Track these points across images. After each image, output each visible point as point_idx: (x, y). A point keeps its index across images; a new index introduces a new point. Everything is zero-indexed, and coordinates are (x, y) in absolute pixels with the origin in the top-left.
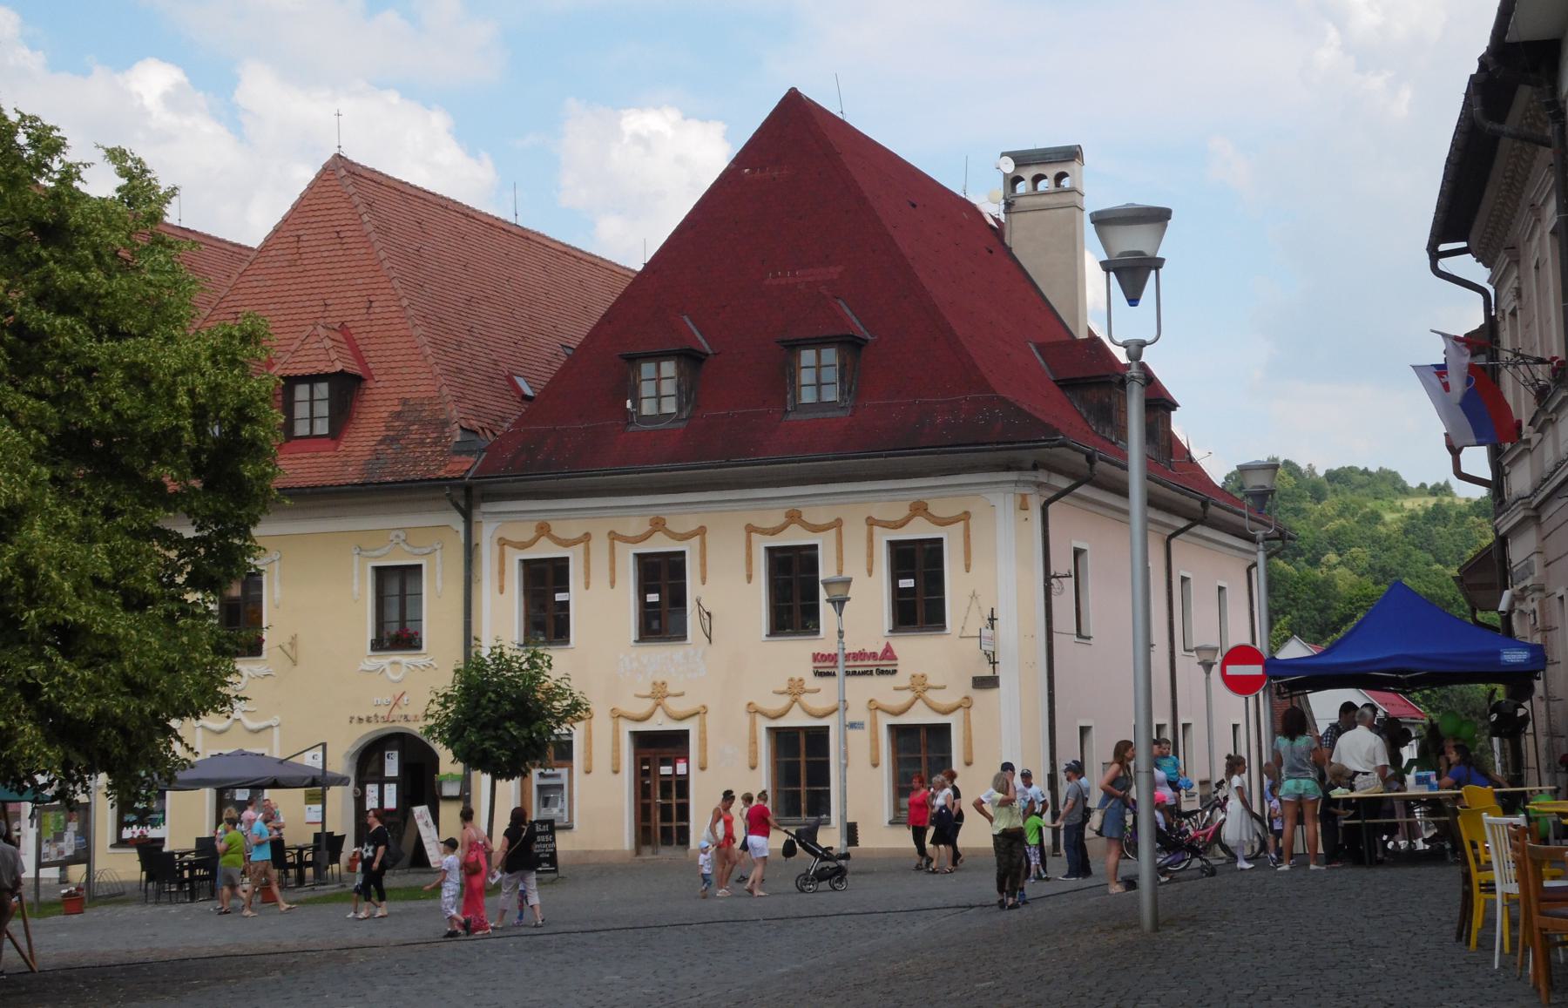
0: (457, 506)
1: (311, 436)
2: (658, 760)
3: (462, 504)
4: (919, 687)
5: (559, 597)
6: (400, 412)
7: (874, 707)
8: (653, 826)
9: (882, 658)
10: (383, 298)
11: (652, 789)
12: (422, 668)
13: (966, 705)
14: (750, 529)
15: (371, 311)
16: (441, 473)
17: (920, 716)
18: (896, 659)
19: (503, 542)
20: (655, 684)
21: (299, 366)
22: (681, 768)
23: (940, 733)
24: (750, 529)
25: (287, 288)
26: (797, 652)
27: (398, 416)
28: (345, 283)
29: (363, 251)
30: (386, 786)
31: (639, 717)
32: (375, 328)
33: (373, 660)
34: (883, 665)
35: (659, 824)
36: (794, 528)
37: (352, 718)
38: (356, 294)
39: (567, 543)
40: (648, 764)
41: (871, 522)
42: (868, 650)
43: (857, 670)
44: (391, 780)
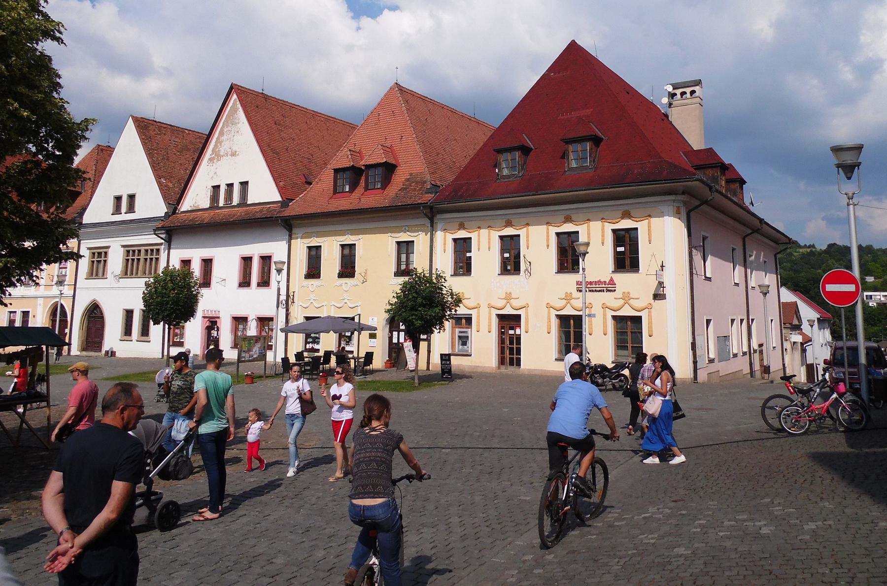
0: (426, 215)
2: (508, 328)
3: (429, 215)
4: (626, 298)
5: (468, 255)
7: (605, 307)
8: (506, 357)
10: (407, 134)
11: (505, 340)
13: (649, 307)
16: (420, 201)
17: (627, 312)
22: (518, 331)
23: (637, 320)
26: (570, 280)
27: (408, 180)
28: (394, 130)
29: (401, 117)
30: (400, 332)
32: (403, 146)
33: (395, 279)
34: (609, 287)
35: (508, 356)
42: (602, 280)
43: (597, 289)
44: (402, 330)
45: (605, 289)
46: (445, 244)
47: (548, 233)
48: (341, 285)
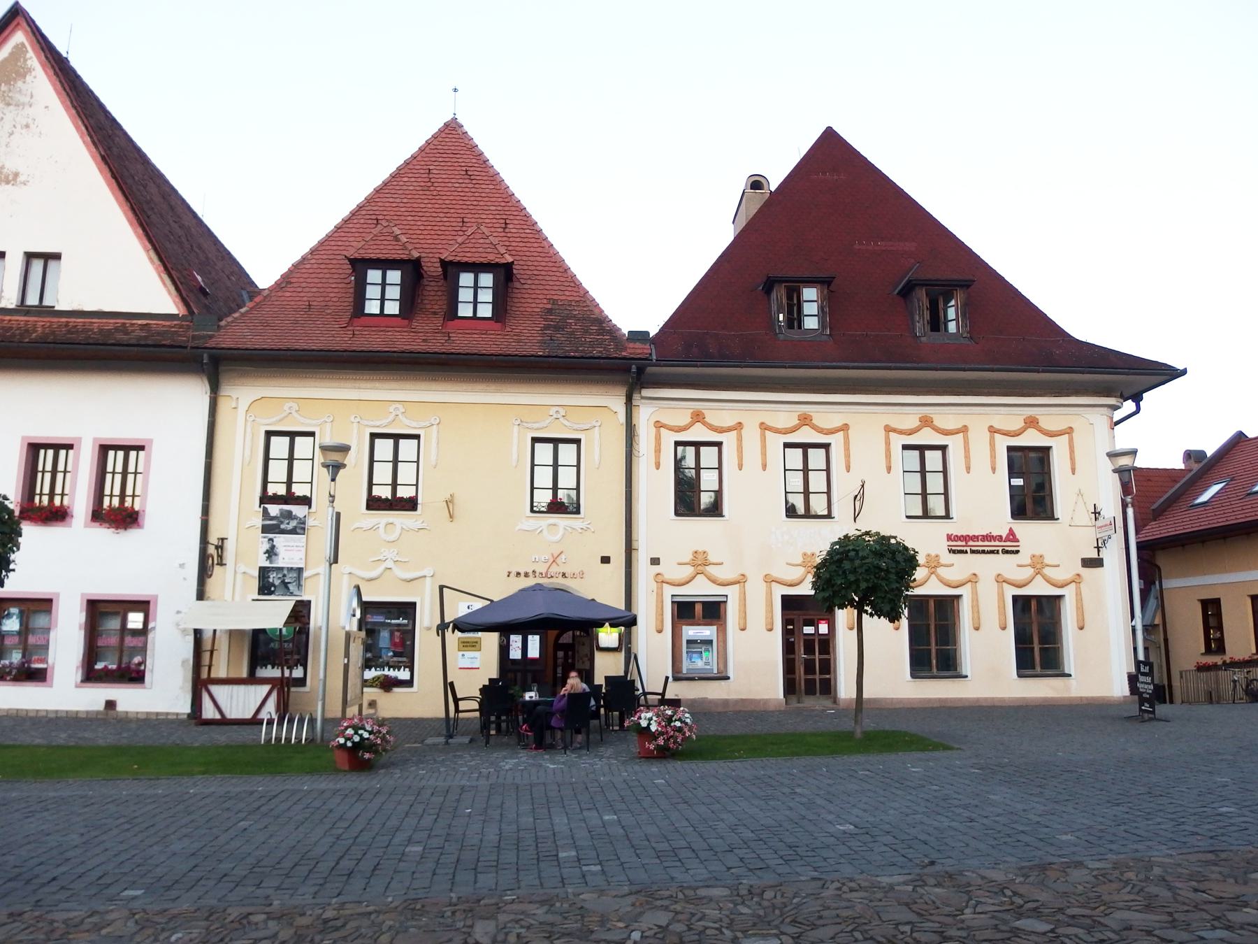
1: (475, 317)
2: (802, 622)
4: (1038, 564)
6: (551, 309)
7: (1001, 580)
9: (1007, 539)
11: (796, 646)
12: (580, 531)
13: (1077, 580)
14: (888, 429)
15: (507, 230)
17: (1039, 588)
18: (1018, 541)
19: (659, 425)
20: (805, 554)
21: (468, 255)
22: (823, 628)
23: (1053, 602)
24: (888, 429)
25: (423, 206)
31: (683, 581)
33: (531, 521)
34: (1008, 545)
36: (927, 430)
37: (509, 573)
38: (491, 216)
39: (721, 430)
40: (793, 625)
41: (993, 430)
42: (994, 534)
43: (986, 549)
45: (1000, 549)
46: (658, 451)
47: (888, 443)
48: (374, 528)
